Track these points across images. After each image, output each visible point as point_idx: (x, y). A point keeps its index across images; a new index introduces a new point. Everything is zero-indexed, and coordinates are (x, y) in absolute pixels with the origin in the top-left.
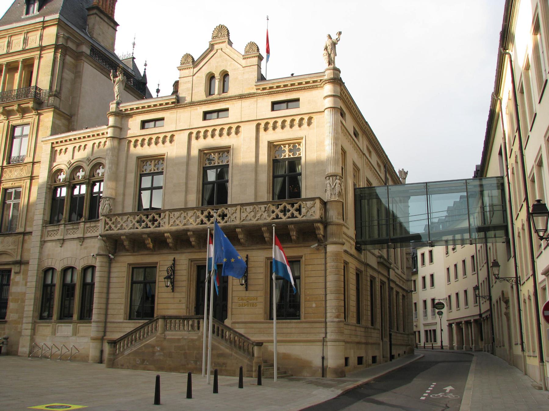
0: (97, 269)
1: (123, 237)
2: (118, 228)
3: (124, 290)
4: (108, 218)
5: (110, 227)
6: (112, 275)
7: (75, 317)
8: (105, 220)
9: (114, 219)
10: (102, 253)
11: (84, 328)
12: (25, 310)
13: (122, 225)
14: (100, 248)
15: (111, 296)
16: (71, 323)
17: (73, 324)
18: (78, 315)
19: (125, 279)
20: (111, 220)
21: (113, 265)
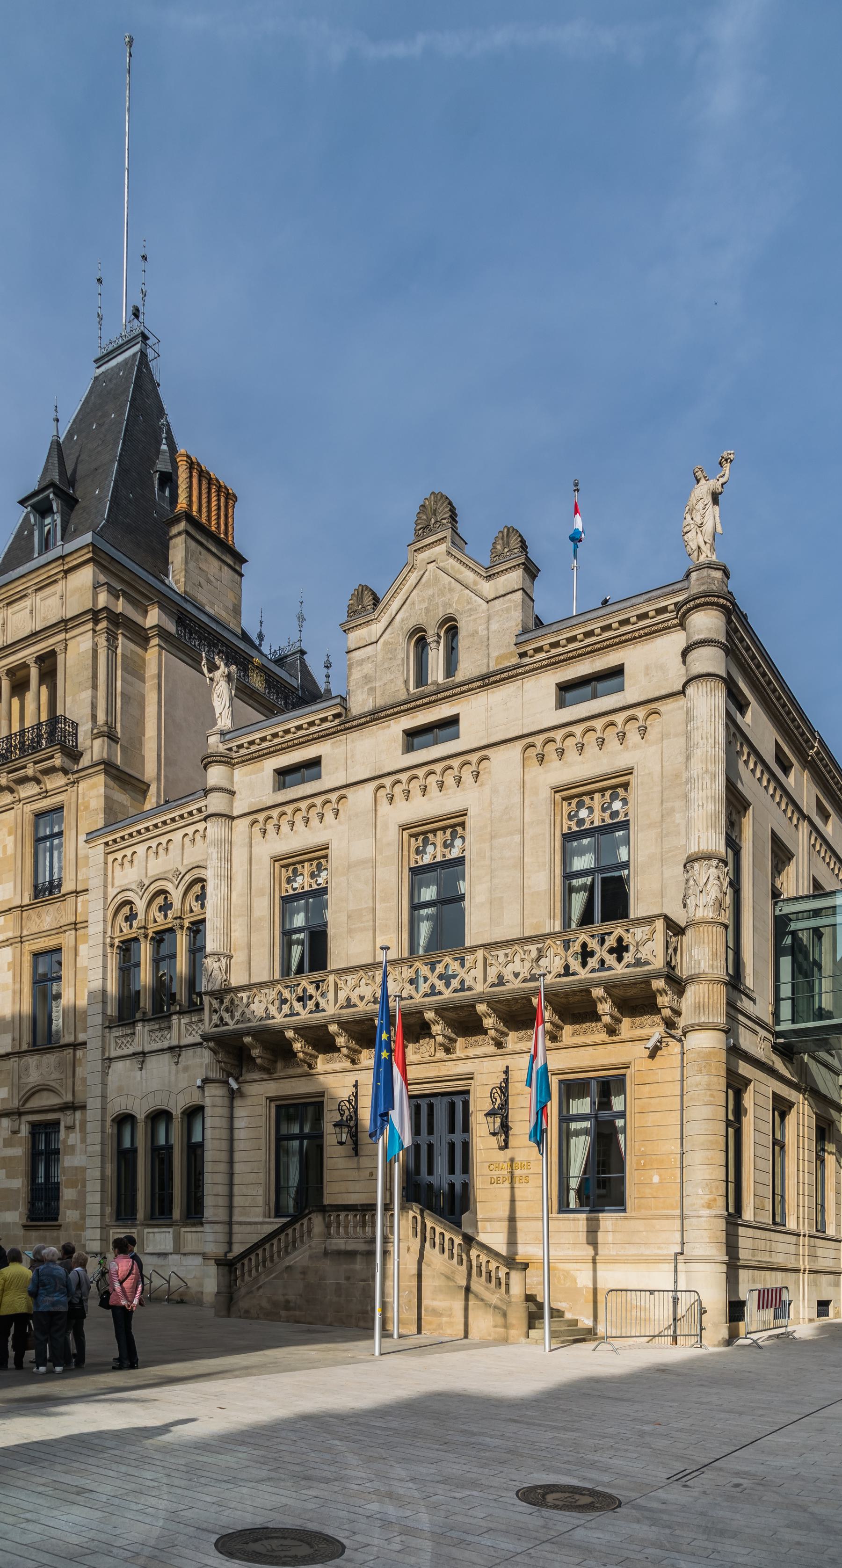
0: (208, 1111)
1: (247, 1040)
2: (236, 1018)
3: (261, 1155)
4: (216, 999)
5: (221, 1019)
6: (238, 1124)
7: (177, 1213)
8: (211, 1004)
9: (227, 1000)
10: (213, 1075)
11: (194, 1235)
12: (87, 1202)
13: (243, 1013)
14: (207, 1066)
15: (238, 1168)
16: (170, 1226)
17: (174, 1228)
18: (181, 1211)
19: (262, 1130)
20: (222, 1002)
21: (237, 1103)
